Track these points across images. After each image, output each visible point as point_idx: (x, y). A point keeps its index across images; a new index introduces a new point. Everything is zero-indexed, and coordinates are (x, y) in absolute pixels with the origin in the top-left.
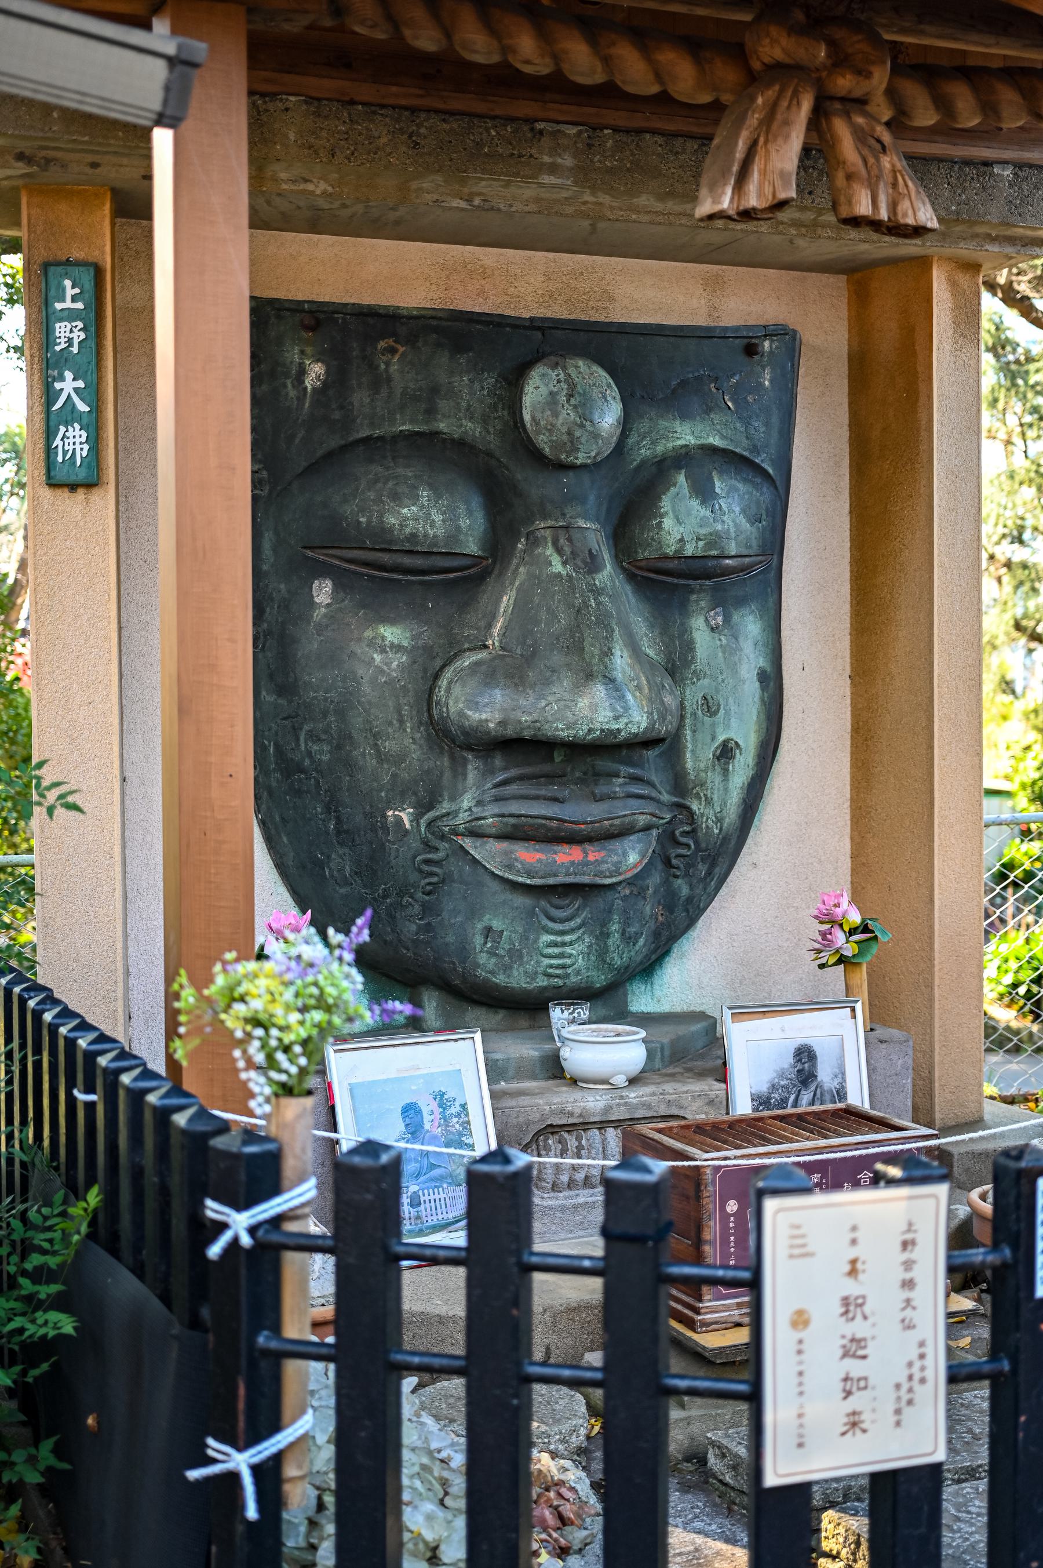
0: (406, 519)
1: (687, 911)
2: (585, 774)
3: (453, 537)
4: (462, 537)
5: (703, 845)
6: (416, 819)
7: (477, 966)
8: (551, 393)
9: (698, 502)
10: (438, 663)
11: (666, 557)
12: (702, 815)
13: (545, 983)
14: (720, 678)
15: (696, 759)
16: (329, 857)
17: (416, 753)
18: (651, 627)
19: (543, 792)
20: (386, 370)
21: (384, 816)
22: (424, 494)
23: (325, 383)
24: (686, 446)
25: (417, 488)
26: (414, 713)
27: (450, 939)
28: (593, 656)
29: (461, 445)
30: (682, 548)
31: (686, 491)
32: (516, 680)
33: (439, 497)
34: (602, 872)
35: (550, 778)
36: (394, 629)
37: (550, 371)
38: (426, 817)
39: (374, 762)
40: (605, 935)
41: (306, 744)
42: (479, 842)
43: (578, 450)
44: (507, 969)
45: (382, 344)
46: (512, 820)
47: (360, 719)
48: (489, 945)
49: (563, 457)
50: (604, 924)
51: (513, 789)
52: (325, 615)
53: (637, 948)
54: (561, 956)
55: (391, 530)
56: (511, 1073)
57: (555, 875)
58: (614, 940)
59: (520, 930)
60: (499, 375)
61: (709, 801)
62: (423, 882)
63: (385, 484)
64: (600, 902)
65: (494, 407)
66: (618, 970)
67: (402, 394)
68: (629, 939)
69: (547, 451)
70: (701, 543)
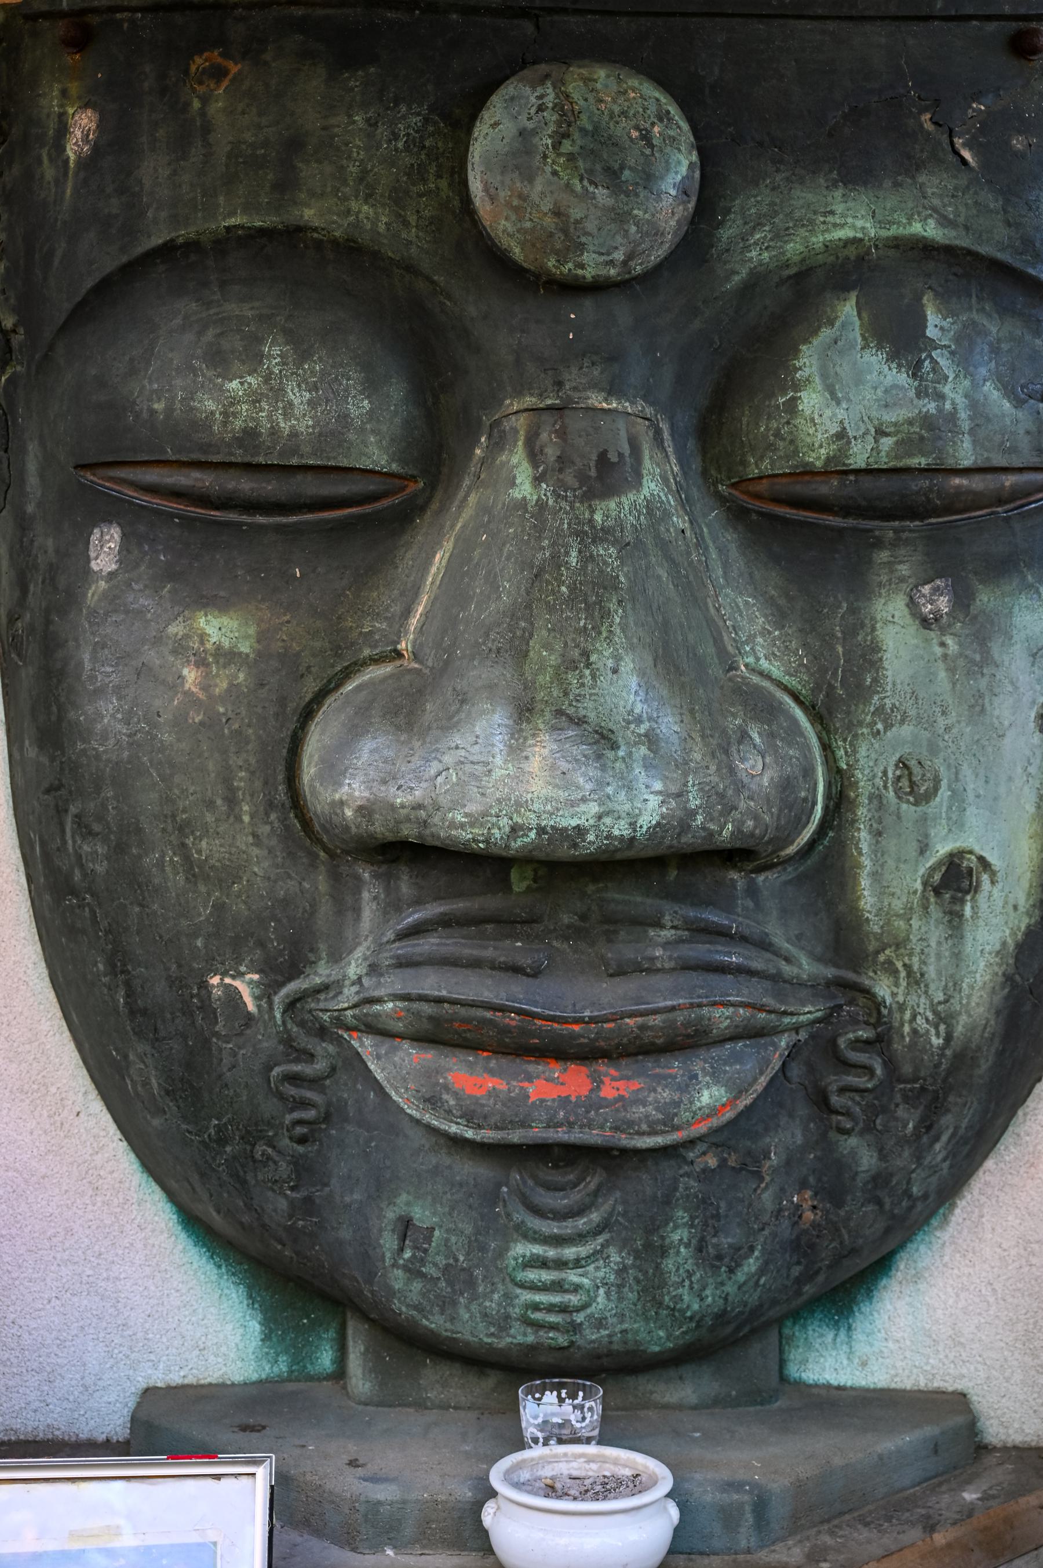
0: (234, 401)
1: (879, 1203)
2: (583, 917)
3: (331, 435)
4: (352, 436)
5: (907, 1069)
6: (266, 992)
7: (391, 1293)
8: (522, 133)
9: (882, 356)
10: (310, 687)
11: (808, 473)
12: (902, 1007)
13: (530, 1339)
14: (942, 722)
15: (882, 890)
16: (126, 1057)
17: (260, 865)
18: (780, 617)
19: (489, 953)
20: (203, 113)
21: (204, 985)
22: (274, 351)
23: (96, 149)
24: (855, 241)
25: (260, 341)
26: (258, 784)
27: (345, 1234)
28: (542, 669)
29: (352, 251)
30: (843, 452)
31: (857, 335)
32: (401, 720)
33: (304, 355)
34: (631, 1123)
35: (505, 924)
36: (225, 620)
37: (528, 90)
38: (284, 992)
39: (181, 878)
40: (652, 1251)
41: (74, 842)
42: (387, 1044)
43: (581, 247)
44: (446, 1304)
45: (198, 62)
46: (427, 1009)
47: (154, 796)
48: (408, 1254)
49: (551, 263)
50: (653, 1226)
51: (428, 944)
52: (105, 595)
53: (740, 1276)
54: (557, 1287)
55: (206, 424)
56: (409, 1530)
57: (524, 1124)
58: (681, 1260)
59: (469, 1229)
60: (432, 109)
61: (916, 979)
62: (288, 1118)
63: (200, 334)
64: (646, 1183)
65: (418, 173)
66: (698, 1320)
67: (229, 156)
68: (713, 1259)
69: (517, 253)
70: (887, 443)
